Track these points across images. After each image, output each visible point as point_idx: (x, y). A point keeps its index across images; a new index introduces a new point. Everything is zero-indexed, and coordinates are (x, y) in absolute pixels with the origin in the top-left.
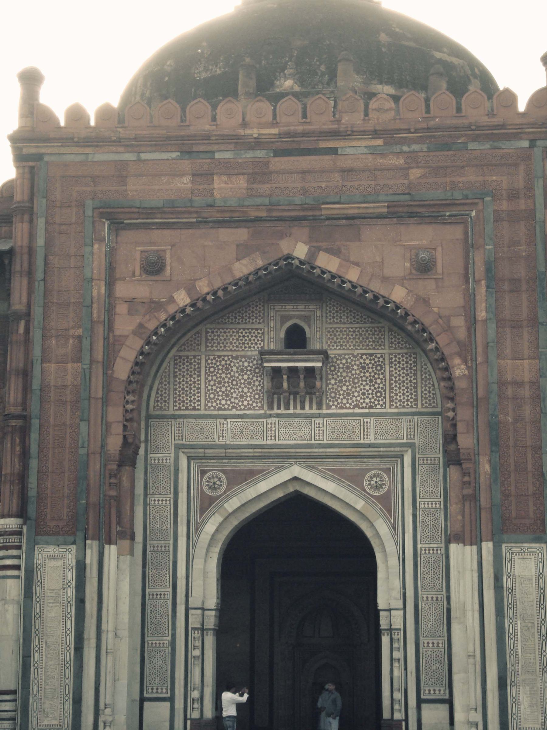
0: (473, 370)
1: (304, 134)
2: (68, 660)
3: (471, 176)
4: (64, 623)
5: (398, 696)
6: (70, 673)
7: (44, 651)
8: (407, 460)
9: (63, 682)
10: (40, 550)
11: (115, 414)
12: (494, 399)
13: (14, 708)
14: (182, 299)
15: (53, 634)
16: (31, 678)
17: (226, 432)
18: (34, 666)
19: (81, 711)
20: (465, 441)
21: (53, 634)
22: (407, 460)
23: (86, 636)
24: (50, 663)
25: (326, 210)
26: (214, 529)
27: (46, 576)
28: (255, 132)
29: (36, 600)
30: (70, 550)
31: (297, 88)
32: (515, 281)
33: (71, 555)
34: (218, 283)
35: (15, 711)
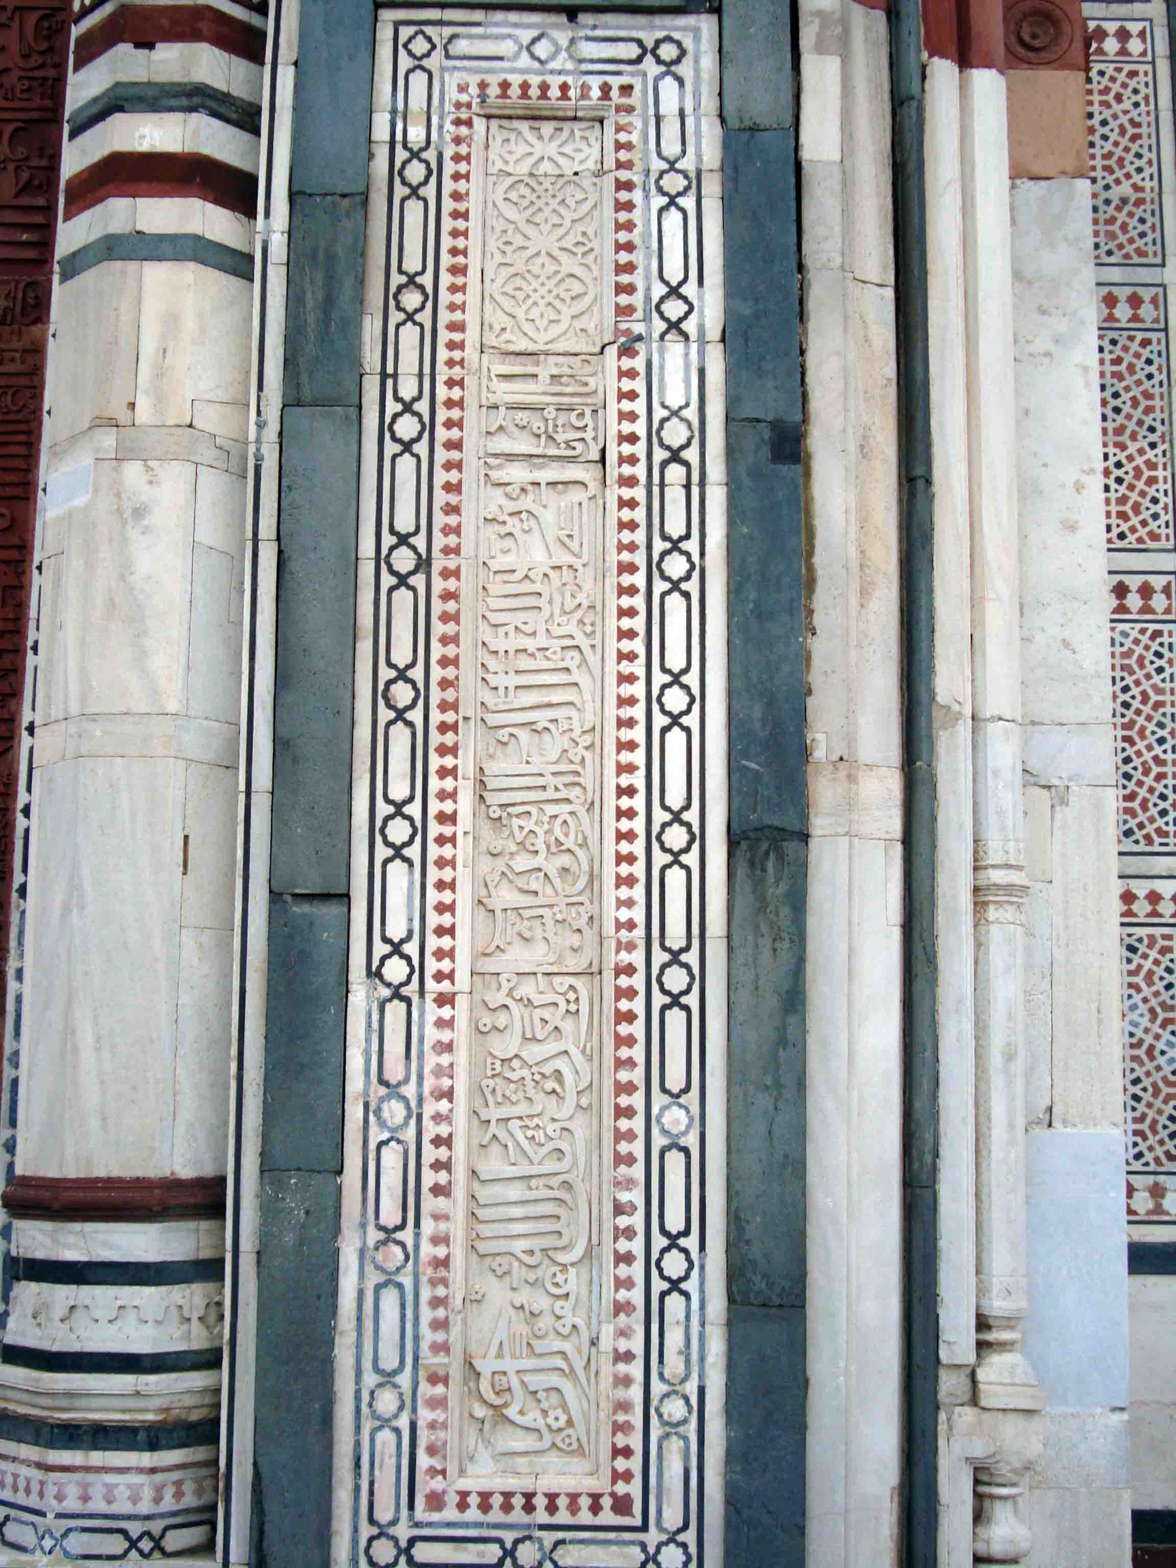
2: (676, 939)
4: (638, 623)
6: (700, 1048)
7: (463, 850)
9: (637, 1124)
10: (420, 46)
13: (196, 1339)
15: (541, 717)
16: (355, 1084)
18: (375, 974)
19: (806, 1382)
21: (541, 717)
23: (822, 743)
24: (519, 957)
27: (473, 243)
29: (385, 429)
30: (668, 52)
35: (209, 1360)
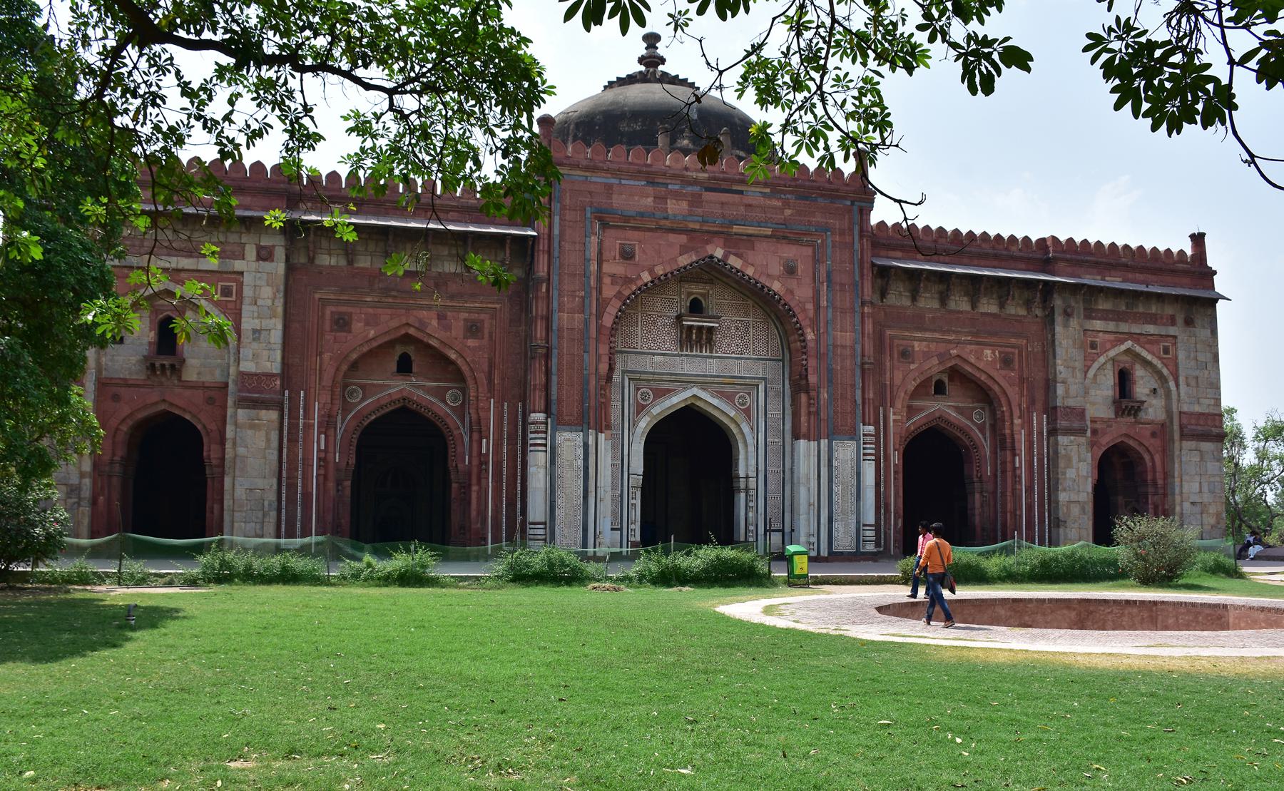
0: (818, 336)
1: (724, 180)
3: (819, 218)
5: (751, 528)
6: (580, 512)
8: (761, 387)
11: (604, 349)
12: (831, 354)
14: (646, 277)
17: (653, 364)
20: (812, 379)
22: (761, 387)
25: (736, 229)
26: (644, 424)
28: (694, 175)
31: (691, 146)
32: (842, 285)
33: (578, 438)
34: (668, 270)
